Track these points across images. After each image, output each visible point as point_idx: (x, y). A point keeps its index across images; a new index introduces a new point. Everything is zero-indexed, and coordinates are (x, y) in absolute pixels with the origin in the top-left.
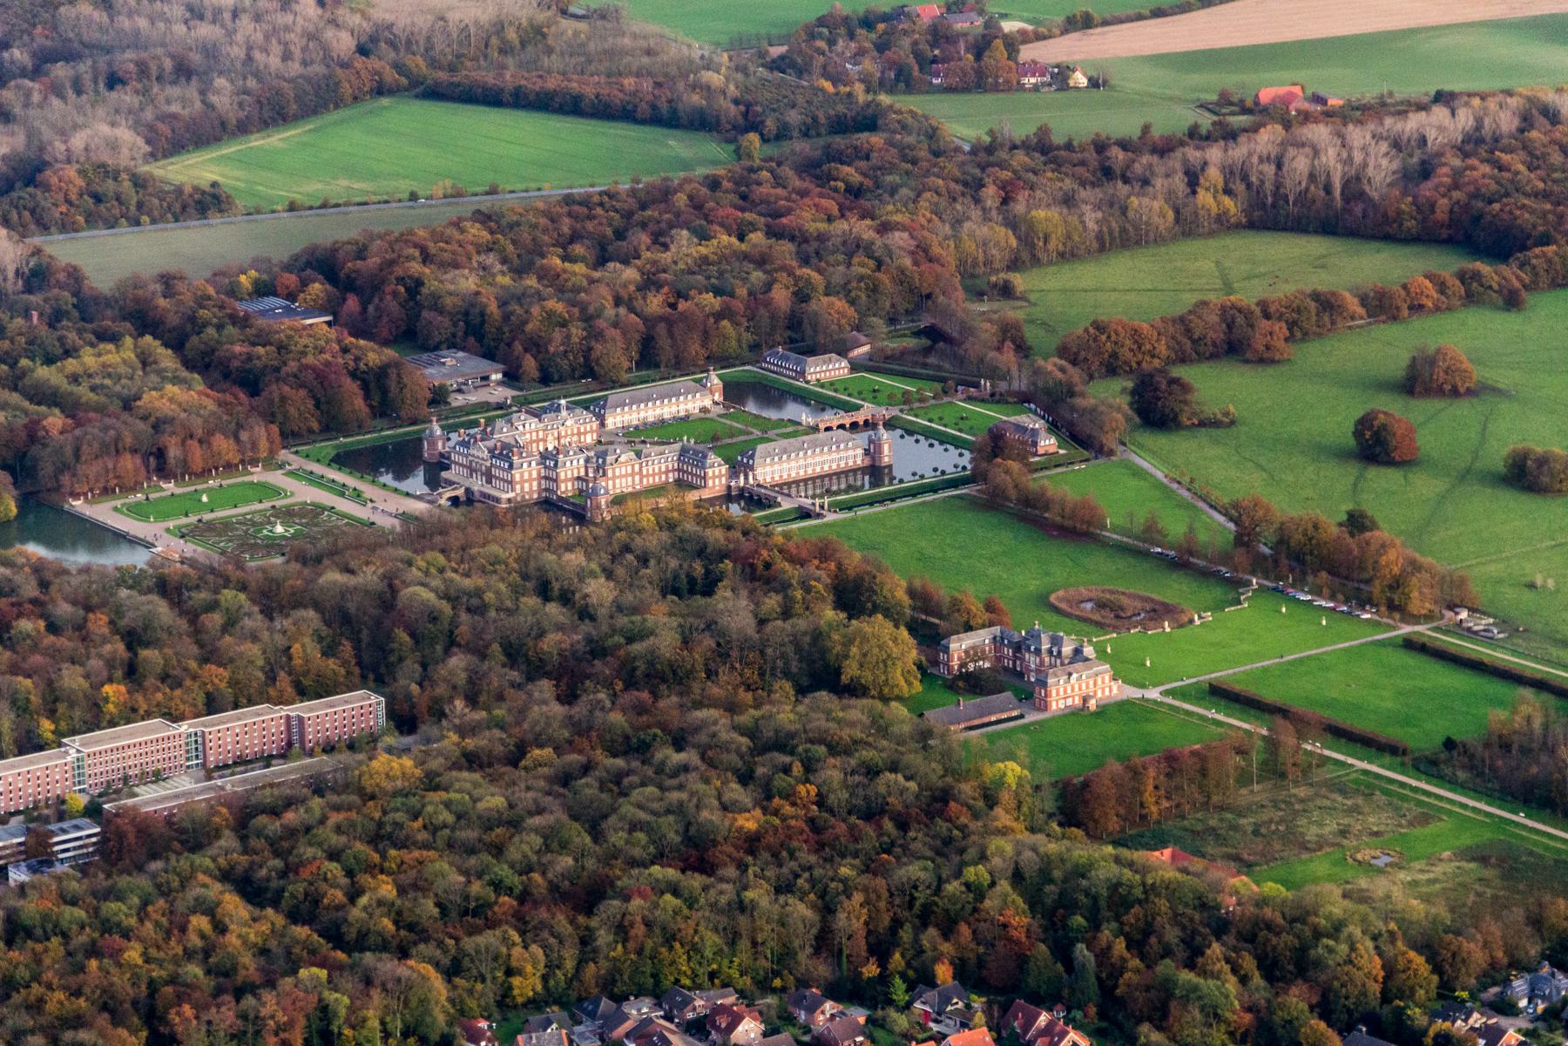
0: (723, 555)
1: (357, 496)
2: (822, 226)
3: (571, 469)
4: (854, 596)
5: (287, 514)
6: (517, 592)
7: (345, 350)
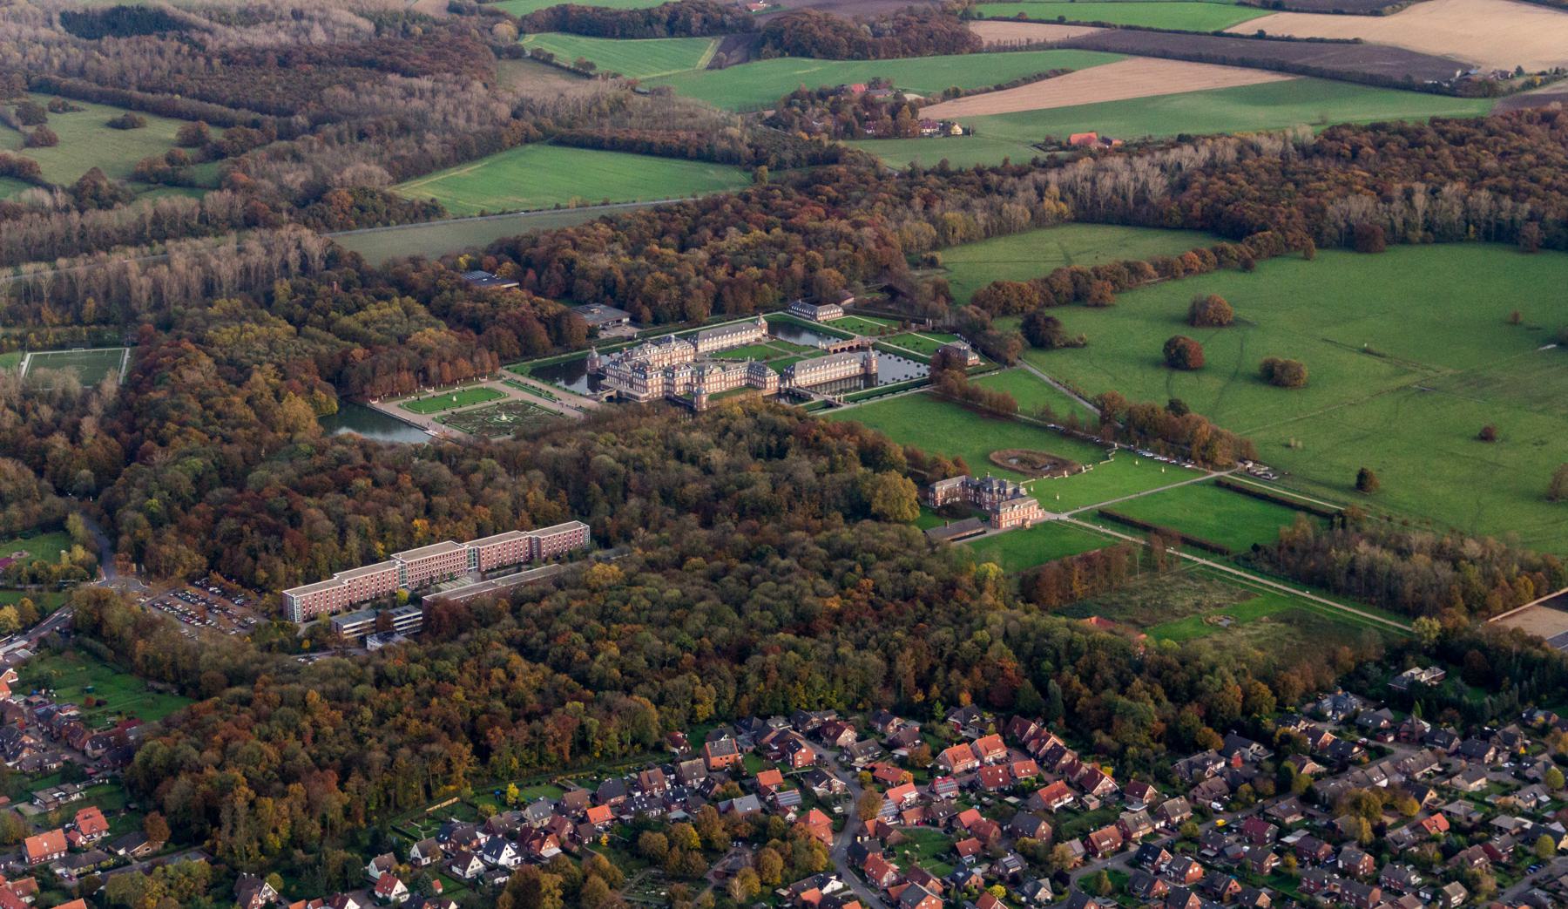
0: (787, 433)
1: (550, 396)
2: (817, 224)
3: (683, 377)
4: (873, 456)
5: (508, 408)
6: (664, 457)
7: (533, 305)
